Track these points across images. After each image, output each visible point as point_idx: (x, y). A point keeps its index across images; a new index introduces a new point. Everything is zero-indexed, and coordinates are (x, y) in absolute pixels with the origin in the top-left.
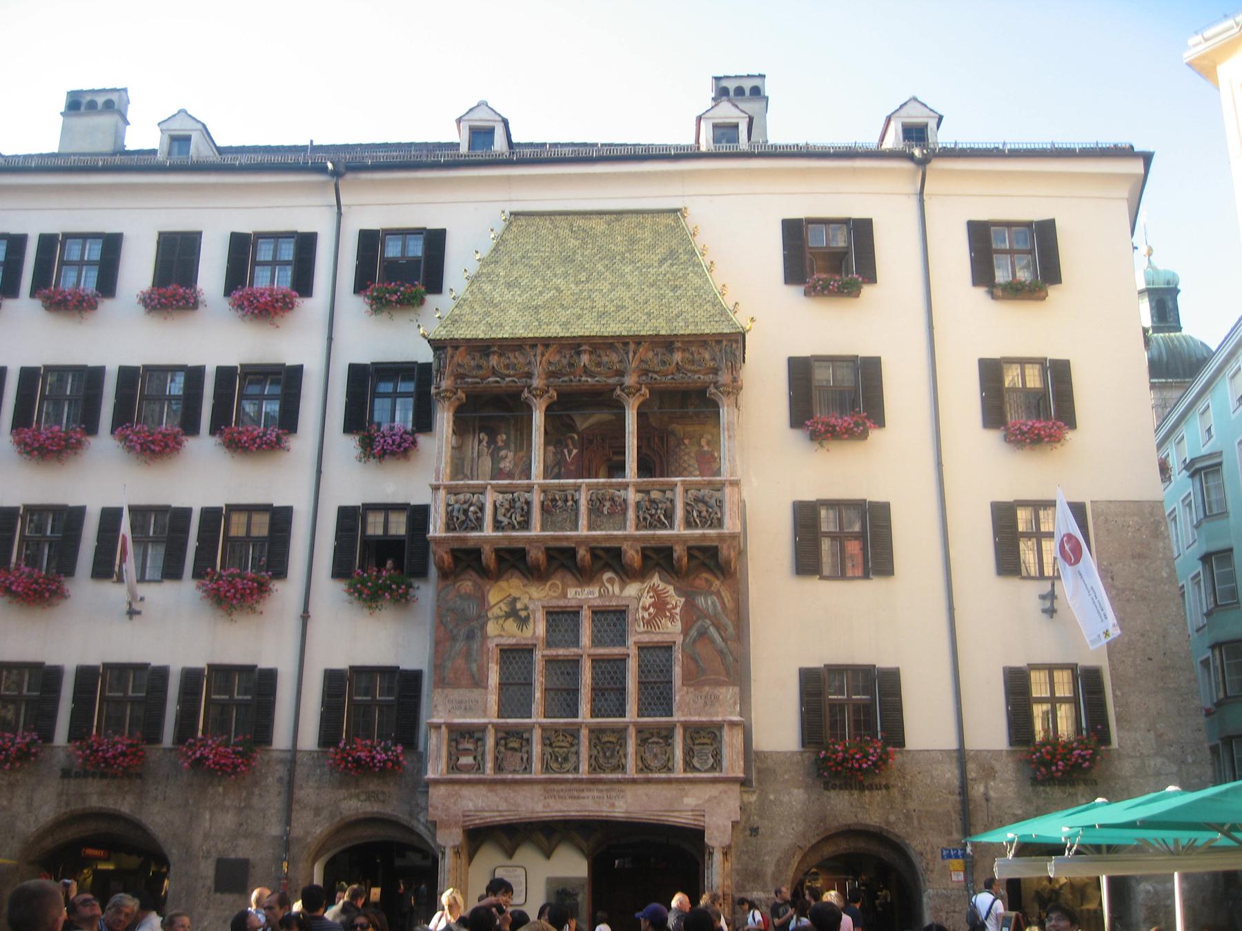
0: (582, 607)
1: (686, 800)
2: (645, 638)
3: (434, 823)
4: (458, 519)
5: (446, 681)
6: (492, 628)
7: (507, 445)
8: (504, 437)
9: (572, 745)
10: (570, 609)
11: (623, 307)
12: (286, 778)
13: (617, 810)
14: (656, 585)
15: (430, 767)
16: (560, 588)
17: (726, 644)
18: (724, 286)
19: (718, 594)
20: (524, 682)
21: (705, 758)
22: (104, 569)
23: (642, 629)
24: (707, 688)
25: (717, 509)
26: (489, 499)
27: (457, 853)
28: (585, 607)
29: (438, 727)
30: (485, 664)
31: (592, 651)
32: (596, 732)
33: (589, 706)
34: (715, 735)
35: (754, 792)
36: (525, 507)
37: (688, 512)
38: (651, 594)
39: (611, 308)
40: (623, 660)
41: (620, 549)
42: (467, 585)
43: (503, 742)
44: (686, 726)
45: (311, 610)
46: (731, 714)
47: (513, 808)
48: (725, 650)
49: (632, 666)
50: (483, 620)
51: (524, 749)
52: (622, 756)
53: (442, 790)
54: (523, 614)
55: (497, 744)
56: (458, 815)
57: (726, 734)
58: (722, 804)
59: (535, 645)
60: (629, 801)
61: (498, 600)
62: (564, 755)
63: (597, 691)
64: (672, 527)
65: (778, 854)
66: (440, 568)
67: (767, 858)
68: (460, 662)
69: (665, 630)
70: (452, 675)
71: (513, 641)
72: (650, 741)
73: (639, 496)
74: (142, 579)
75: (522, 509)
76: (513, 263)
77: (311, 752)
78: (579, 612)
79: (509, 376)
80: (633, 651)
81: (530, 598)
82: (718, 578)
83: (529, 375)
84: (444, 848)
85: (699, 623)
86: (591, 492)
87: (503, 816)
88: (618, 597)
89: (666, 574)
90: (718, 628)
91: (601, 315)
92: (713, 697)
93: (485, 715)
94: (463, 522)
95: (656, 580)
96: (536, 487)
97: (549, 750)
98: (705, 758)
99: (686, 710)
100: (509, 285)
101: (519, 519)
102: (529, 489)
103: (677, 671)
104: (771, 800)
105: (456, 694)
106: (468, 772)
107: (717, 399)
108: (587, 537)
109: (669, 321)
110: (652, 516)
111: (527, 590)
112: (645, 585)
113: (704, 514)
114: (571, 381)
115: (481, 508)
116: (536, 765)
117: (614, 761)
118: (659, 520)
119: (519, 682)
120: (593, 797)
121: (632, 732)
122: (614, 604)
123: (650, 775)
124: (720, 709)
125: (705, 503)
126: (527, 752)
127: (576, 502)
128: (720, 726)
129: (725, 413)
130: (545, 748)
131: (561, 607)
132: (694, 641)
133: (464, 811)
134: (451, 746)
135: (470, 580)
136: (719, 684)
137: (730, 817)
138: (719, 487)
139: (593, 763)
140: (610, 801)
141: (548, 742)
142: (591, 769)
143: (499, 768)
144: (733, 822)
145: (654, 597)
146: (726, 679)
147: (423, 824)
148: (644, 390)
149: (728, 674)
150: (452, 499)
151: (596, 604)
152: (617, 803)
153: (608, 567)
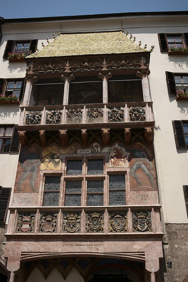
0: (84, 157)
1: (135, 246)
2: (112, 170)
3: (6, 258)
4: (31, 120)
5: (20, 189)
8: (54, 101)
9: (77, 219)
10: (78, 159)
13: (100, 252)
14: (117, 148)
15: (8, 230)
16: (74, 149)
17: (151, 173)
18: (140, 42)
20: (56, 191)
21: (144, 225)
24: (142, 192)
25: (143, 113)
28: (85, 157)
30: (39, 182)
32: (89, 212)
33: (86, 200)
34: (148, 214)
35: (167, 244)
36: (60, 115)
37: (130, 115)
38: (115, 151)
41: (100, 130)
43: (44, 217)
46: (155, 203)
47: (47, 251)
48: (150, 175)
51: (54, 221)
52: (102, 224)
55: (41, 218)
56: (19, 254)
58: (153, 248)
59: (61, 174)
60: (106, 247)
61: (47, 155)
62: (74, 224)
63: (89, 195)
65: (183, 277)
67: (177, 279)
68: (27, 181)
69: (122, 166)
70: (23, 187)
71: (52, 172)
72: (115, 217)
73: (108, 110)
75: (58, 115)
78: (82, 160)
79: (56, 69)
80: (107, 176)
81: (61, 154)
82: (144, 144)
84: (10, 272)
85: (137, 163)
86: (87, 109)
87: (42, 255)
88: (100, 153)
89: (121, 143)
90: (146, 165)
92: (145, 196)
94: (33, 121)
95: (117, 146)
96: (64, 107)
97: (66, 221)
98: (144, 225)
99: (133, 202)
101: (56, 119)
103: (128, 183)
104: (176, 248)
105: (23, 195)
106: (26, 232)
107: (140, 75)
110: (115, 117)
111: (59, 150)
112: (112, 148)
113: (138, 115)
114: (81, 70)
115: (41, 116)
116: (59, 227)
117: (97, 227)
118: (118, 118)
119: (54, 191)
120: (87, 245)
122: (98, 156)
123: (116, 234)
124: (149, 201)
125: (139, 112)
126: (55, 222)
127: (81, 113)
129: (144, 81)
130: (64, 220)
131: (74, 158)
132: (135, 171)
133: (22, 252)
134: (19, 219)
135: (34, 147)
137: (158, 256)
139: (87, 226)
140: (96, 247)
141: (65, 217)
142: (87, 230)
144: (159, 258)
145: (116, 153)
146: (152, 188)
147: (3, 260)
149: (152, 185)
150: (27, 112)
151: (90, 156)
152: (99, 248)
153: (95, 140)
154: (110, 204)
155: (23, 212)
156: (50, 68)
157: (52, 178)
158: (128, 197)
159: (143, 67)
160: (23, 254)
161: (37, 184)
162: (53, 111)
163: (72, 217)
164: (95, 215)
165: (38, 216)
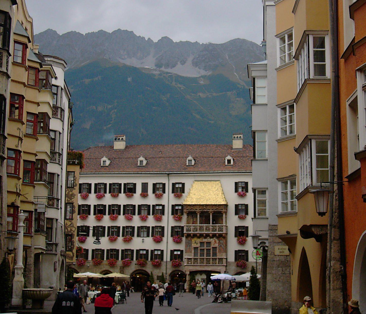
2: (213, 246)
6: (193, 245)
7: (195, 217)
11: (210, 199)
12: (166, 265)
19: (223, 240)
22: (139, 235)
23: (213, 245)
26: (192, 227)
27: (189, 275)
29: (185, 258)
31: (207, 248)
39: (208, 199)
40: (210, 249)
42: (189, 239)
44: (218, 258)
45: (168, 242)
49: (211, 250)
50: (191, 243)
53: (187, 266)
54: (197, 243)
57: (223, 259)
63: (207, 254)
64: (216, 231)
66: (186, 236)
71: (195, 247)
74: (144, 237)
76: (195, 190)
77: (169, 261)
80: (212, 248)
83: (197, 209)
90: (223, 245)
91: (207, 200)
93: (192, 257)
95: (215, 238)
100: (194, 194)
102: (197, 226)
103: (217, 251)
105: (188, 254)
108: (205, 233)
109: (216, 202)
116: (199, 263)
121: (211, 259)
128: (223, 258)
136: (223, 253)
138: (223, 226)
143: (194, 264)
148: (213, 212)
153: (208, 237)
154: (213, 256)
155: (189, 259)
156: (192, 209)
157: (196, 248)
158: (217, 255)
159: (223, 210)
160: (190, 270)
161: (192, 251)
162: (194, 227)
163: (202, 260)
164: (208, 260)
165: (193, 260)
